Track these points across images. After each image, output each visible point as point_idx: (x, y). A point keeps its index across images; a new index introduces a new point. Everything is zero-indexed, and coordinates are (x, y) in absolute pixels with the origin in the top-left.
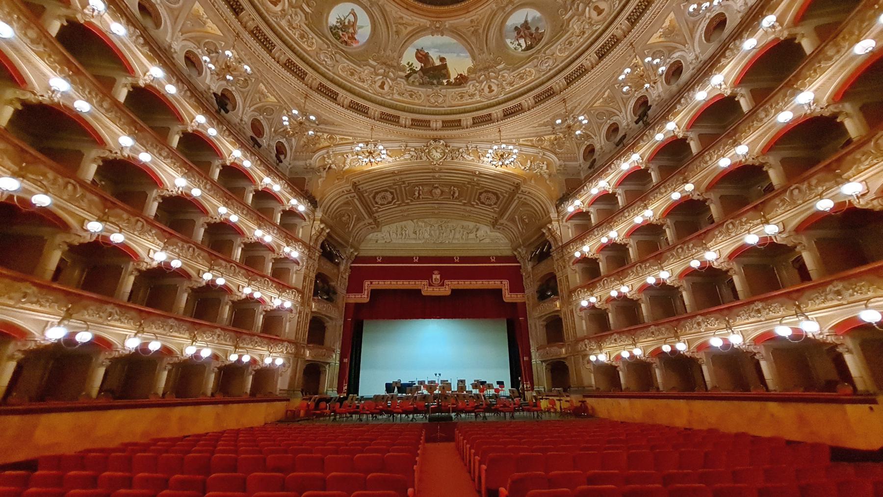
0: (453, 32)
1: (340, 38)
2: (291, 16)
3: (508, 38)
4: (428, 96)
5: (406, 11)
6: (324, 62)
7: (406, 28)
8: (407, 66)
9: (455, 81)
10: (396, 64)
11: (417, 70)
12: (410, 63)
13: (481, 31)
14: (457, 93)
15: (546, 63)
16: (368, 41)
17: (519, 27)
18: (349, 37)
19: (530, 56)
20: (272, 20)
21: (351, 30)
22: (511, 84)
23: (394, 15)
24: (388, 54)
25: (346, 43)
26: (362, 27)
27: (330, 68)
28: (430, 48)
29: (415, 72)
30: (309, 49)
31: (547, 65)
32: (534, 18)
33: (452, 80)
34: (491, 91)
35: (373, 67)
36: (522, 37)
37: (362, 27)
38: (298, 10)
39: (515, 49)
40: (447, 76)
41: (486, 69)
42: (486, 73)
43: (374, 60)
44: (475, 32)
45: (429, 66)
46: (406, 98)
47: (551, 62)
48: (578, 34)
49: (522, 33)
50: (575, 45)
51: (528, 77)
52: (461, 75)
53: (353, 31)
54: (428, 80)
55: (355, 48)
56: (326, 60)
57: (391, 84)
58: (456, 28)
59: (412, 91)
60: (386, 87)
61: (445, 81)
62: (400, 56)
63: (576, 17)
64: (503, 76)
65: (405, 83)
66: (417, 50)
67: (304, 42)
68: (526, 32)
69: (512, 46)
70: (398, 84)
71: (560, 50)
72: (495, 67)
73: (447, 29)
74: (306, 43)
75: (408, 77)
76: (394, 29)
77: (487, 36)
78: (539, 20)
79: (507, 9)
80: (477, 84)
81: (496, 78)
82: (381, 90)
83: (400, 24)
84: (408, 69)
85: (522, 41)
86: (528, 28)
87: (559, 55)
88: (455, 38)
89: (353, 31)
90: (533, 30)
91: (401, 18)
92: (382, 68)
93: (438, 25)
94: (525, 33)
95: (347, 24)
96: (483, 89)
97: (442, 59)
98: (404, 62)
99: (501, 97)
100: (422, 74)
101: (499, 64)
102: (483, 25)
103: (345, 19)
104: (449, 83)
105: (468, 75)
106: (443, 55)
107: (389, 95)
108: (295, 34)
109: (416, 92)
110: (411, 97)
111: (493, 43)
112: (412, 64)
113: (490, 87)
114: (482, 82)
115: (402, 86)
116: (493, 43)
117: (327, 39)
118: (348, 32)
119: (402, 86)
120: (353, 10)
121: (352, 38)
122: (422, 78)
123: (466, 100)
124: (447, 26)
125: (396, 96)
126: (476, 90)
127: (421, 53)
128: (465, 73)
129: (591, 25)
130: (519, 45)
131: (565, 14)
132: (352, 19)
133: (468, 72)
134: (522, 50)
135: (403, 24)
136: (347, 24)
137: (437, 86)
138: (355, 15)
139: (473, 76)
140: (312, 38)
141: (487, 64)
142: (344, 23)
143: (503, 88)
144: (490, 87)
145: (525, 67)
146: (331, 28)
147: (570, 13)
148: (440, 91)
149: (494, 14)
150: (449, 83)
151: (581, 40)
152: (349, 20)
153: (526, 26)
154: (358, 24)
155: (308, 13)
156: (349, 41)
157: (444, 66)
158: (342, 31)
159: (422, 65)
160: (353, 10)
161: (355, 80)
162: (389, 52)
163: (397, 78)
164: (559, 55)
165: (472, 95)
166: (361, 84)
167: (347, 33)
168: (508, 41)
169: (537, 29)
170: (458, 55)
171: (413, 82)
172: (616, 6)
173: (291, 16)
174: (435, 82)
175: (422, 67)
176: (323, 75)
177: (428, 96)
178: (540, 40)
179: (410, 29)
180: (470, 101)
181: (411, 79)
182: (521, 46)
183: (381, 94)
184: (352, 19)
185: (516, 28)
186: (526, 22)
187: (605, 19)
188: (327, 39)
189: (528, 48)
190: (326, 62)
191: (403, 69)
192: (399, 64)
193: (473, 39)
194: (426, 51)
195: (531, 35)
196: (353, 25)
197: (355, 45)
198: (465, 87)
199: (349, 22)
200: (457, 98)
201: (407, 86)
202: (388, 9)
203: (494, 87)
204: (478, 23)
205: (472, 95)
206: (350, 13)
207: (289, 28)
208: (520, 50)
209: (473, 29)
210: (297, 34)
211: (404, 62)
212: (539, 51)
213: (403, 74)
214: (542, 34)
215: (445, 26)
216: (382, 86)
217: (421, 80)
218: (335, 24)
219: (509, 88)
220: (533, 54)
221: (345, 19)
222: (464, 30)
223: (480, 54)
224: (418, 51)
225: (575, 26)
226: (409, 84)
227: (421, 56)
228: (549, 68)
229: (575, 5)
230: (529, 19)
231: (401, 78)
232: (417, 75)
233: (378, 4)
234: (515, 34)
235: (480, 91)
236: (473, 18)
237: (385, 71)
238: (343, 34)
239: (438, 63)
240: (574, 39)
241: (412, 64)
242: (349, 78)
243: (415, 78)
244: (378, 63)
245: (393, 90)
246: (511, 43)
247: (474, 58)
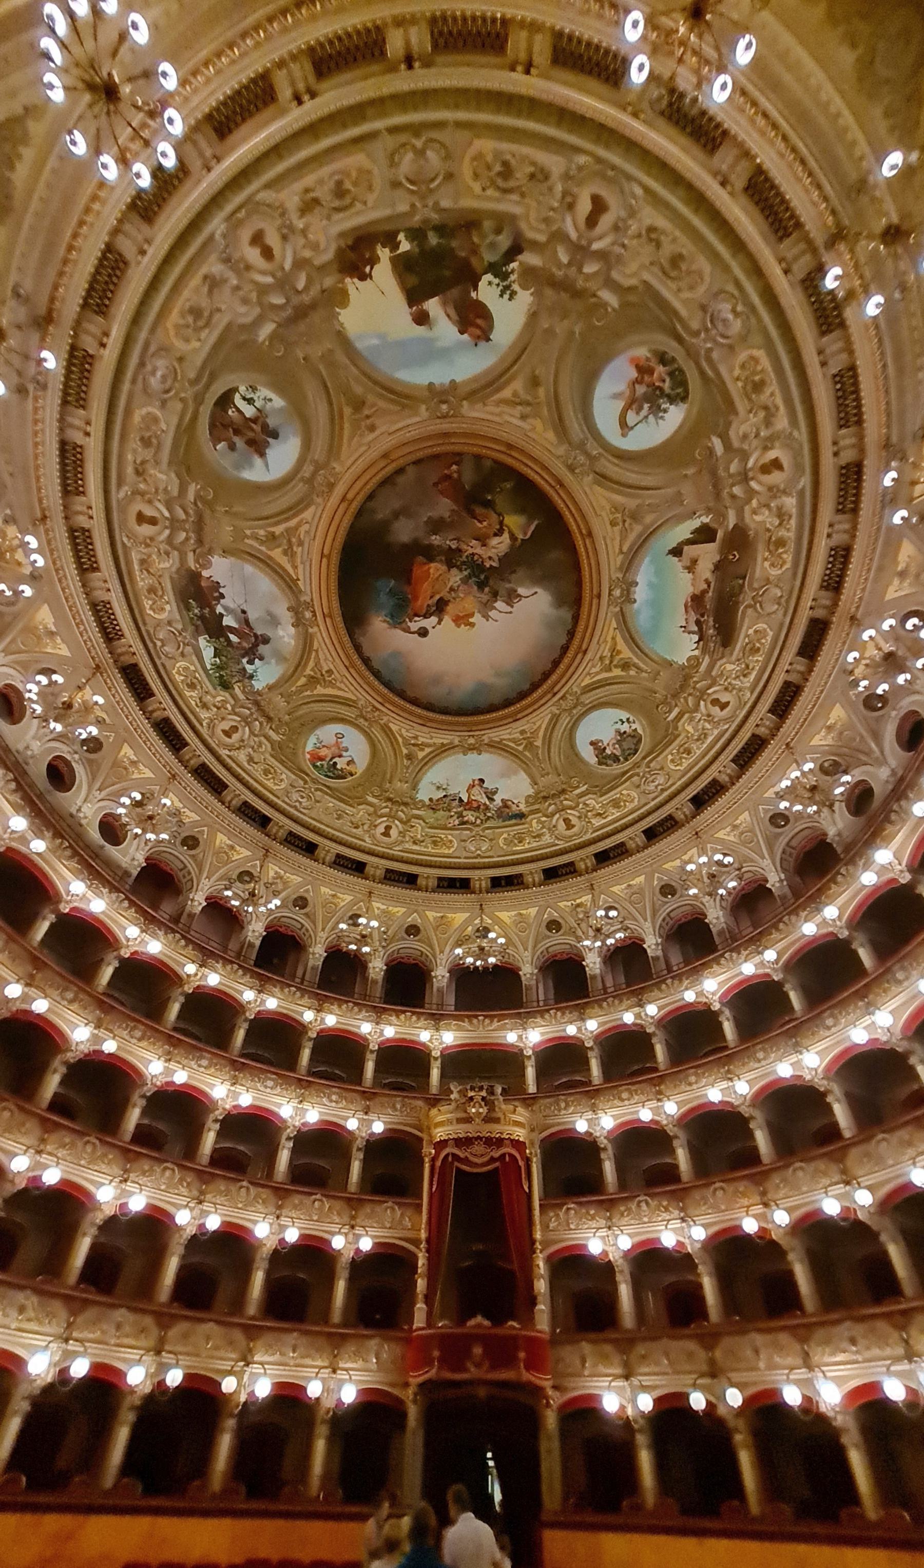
0: (407, 397)
1: (671, 374)
2: (757, 435)
3: (281, 410)
4: (449, 176)
5: (512, 440)
6: (739, 308)
7: (515, 394)
8: (516, 287)
9: (374, 251)
10: (549, 292)
11: (488, 277)
12: (506, 296)
13: (347, 411)
14: (359, 206)
15: (164, 377)
16: (607, 358)
17: (270, 440)
18: (651, 372)
19: (213, 377)
20: (802, 434)
21: (641, 390)
22: (213, 283)
23: (538, 423)
24: (566, 322)
25: (663, 359)
26: (616, 396)
27: (731, 288)
28: (460, 346)
29: (498, 270)
30: (760, 354)
31: (159, 374)
32: (251, 465)
33: (384, 254)
34: (257, 239)
35: (611, 284)
36: (255, 420)
37: (616, 396)
38: (736, 444)
39: (254, 389)
40: (402, 266)
41: (301, 313)
42: (296, 300)
43: (605, 305)
44: (358, 405)
45: (455, 292)
46: (524, 159)
47: (155, 382)
48: (148, 466)
49: (257, 428)
50: (134, 443)
51: (181, 322)
52: (363, 277)
53: (637, 386)
54: (454, 244)
55: (641, 343)
56: (730, 316)
57: (569, 220)
58: (404, 406)
59: (506, 191)
60: (584, 207)
61: (405, 246)
62: (533, 316)
63: (175, 493)
64: (245, 301)
65: (523, 226)
66: (488, 339)
67: (762, 371)
68: (251, 434)
69: (264, 392)
70: (546, 220)
71: (156, 420)
72: (279, 325)
73: (423, 402)
74: (759, 368)
75: (515, 251)
76: (541, 391)
77: (330, 404)
78: (239, 466)
79: (312, 468)
80: (307, 254)
81: (263, 290)
82: (604, 193)
83: (528, 404)
84: (513, 277)
85: (249, 411)
86: (251, 443)
87: (150, 409)
88: (397, 381)
89: (637, 386)
90: (239, 442)
91: (523, 417)
92: (588, 277)
93: (444, 407)
94: (253, 430)
95: (646, 406)
96: (285, 238)
97: (422, 319)
98: (525, 298)
99: (216, 225)
100: (474, 262)
101: (273, 337)
102: (347, 425)
103: (646, 417)
104: (390, 240)
105: (342, 281)
106: (421, 330)
107: (580, 168)
108: (772, 394)
109: (490, 192)
110: (505, 164)
111: (311, 389)
112: (501, 296)
113: (267, 253)
114: (300, 264)
115: (533, 215)
116: (311, 389)
117: (702, 373)
118: (648, 386)
119: (533, 215)
120: (624, 435)
121: (643, 370)
122: (475, 251)
123: (321, 182)
124: (423, 407)
125: (554, 163)
126: (304, 232)
127: (478, 332)
128: (352, 284)
129: (136, 492)
130: (250, 401)
131: (197, 493)
132: (631, 418)
133: (344, 293)
134: (236, 390)
135: (520, 404)
136: (646, 406)
137: (426, 221)
138: (624, 425)
139: (329, 281)
140: (738, 379)
141: (302, 327)
142: (650, 408)
143: (227, 260)
144: (267, 253)
145: (207, 348)
146: (684, 399)
147: (191, 496)
148: (413, 206)
149: (333, 450)
150: (390, 240)
151: (130, 457)
152: (638, 413)
153: (258, 447)
154: (620, 404)
155: (720, 436)
156: (653, 363)
157: (414, 297)
158: (661, 389)
159: (473, 295)
160: (624, 435)
161: (674, 240)
162: (561, 328)
163: (549, 241)
164: (150, 409)
165: (309, 205)
166: (661, 222)
167: (651, 385)
168: (278, 402)
169: (232, 447)
170: (382, 337)
171: (498, 231)
172: (125, 540)
173: (757, 435)
174: (433, 240)
175: (476, 288)
176: (757, 271)
177: (449, 176)
178: (212, 426)
179: (507, 393)
180: (309, 180)
181: (504, 241)
182: (244, 399)
183: (604, 177)
184: (631, 418)
185: (275, 435)
186: (262, 454)
187: (123, 511)
188: (702, 373)
189: (225, 400)
190: (734, 311)
191: (530, 276)
192: (537, 294)
193: (358, 390)
194: (466, 335)
195: (237, 432)
196: (633, 403)
197: (642, 352)
198: (342, 235)
199: (640, 408)
200: (355, 184)
201: (517, 210)
202: (551, 435)
203: (253, 255)
204: (359, 428)
205: (309, 205)
206: (632, 428)
207: (777, 409)
208: (242, 389)
209: (366, 412)
210: (768, 393)
211: (525, 298)
212: (199, 400)
213: (530, 258)
214: (216, 440)
215: (427, 409)
216: (599, 206)
217: (476, 239)
218: (672, 407)
219: (213, 266)
220: (208, 386)
221: (646, 417)
222: (382, 404)
223: (331, 351)
224: (484, 335)
225: (164, 477)
226: (513, 218)
227: (479, 321)
228: (149, 367)
229: (191, 512)
230: (258, 461)
231: (535, 246)
232: (489, 257)
233: (570, 444)
234: (272, 422)
235: (291, 228)
236: (371, 436)
237: (580, 270)
238: (664, 381)
239: (433, 305)
240: (148, 454)
241: (501, 296)
242: (685, 246)
243: (493, 246)
244: (594, 295)
245: (565, 193)
246: (270, 400)
247: (342, 338)
